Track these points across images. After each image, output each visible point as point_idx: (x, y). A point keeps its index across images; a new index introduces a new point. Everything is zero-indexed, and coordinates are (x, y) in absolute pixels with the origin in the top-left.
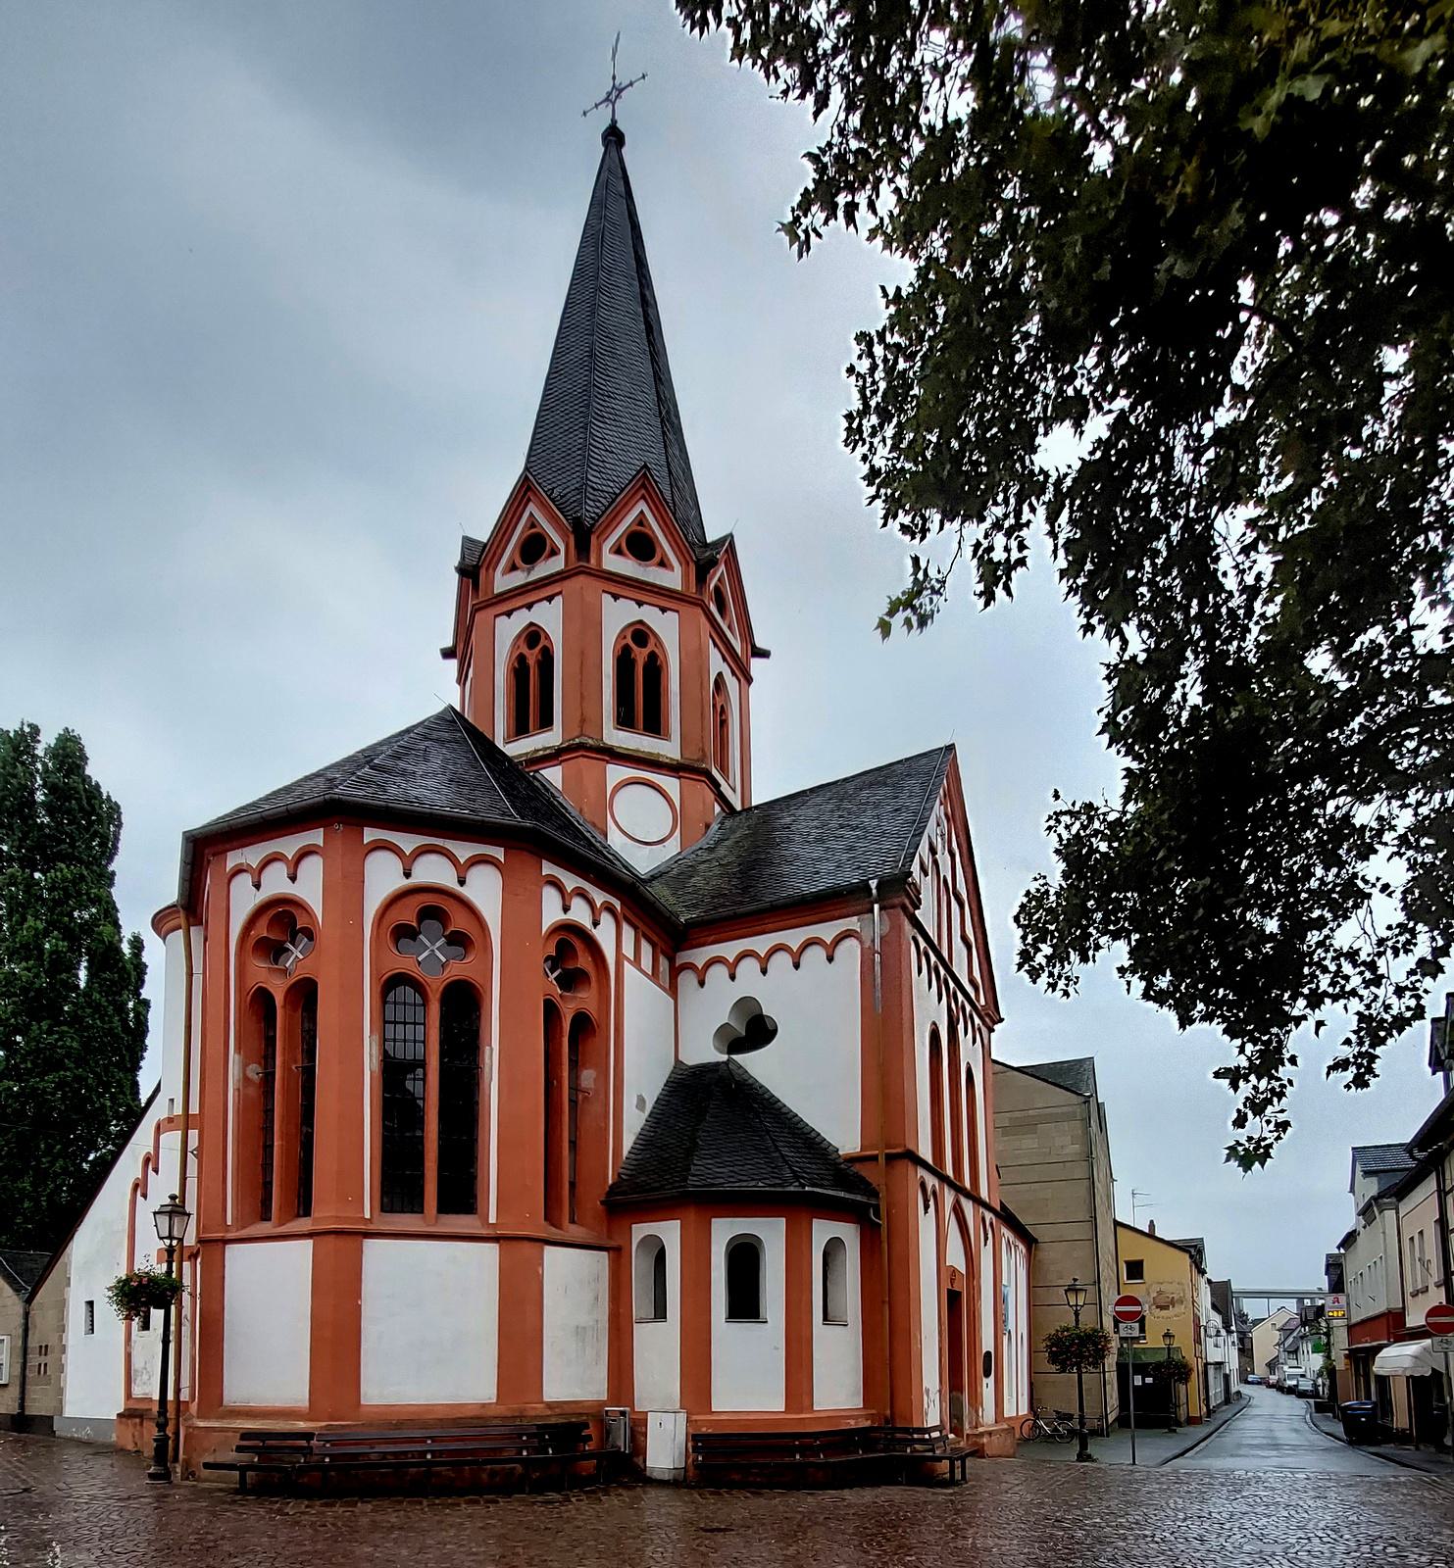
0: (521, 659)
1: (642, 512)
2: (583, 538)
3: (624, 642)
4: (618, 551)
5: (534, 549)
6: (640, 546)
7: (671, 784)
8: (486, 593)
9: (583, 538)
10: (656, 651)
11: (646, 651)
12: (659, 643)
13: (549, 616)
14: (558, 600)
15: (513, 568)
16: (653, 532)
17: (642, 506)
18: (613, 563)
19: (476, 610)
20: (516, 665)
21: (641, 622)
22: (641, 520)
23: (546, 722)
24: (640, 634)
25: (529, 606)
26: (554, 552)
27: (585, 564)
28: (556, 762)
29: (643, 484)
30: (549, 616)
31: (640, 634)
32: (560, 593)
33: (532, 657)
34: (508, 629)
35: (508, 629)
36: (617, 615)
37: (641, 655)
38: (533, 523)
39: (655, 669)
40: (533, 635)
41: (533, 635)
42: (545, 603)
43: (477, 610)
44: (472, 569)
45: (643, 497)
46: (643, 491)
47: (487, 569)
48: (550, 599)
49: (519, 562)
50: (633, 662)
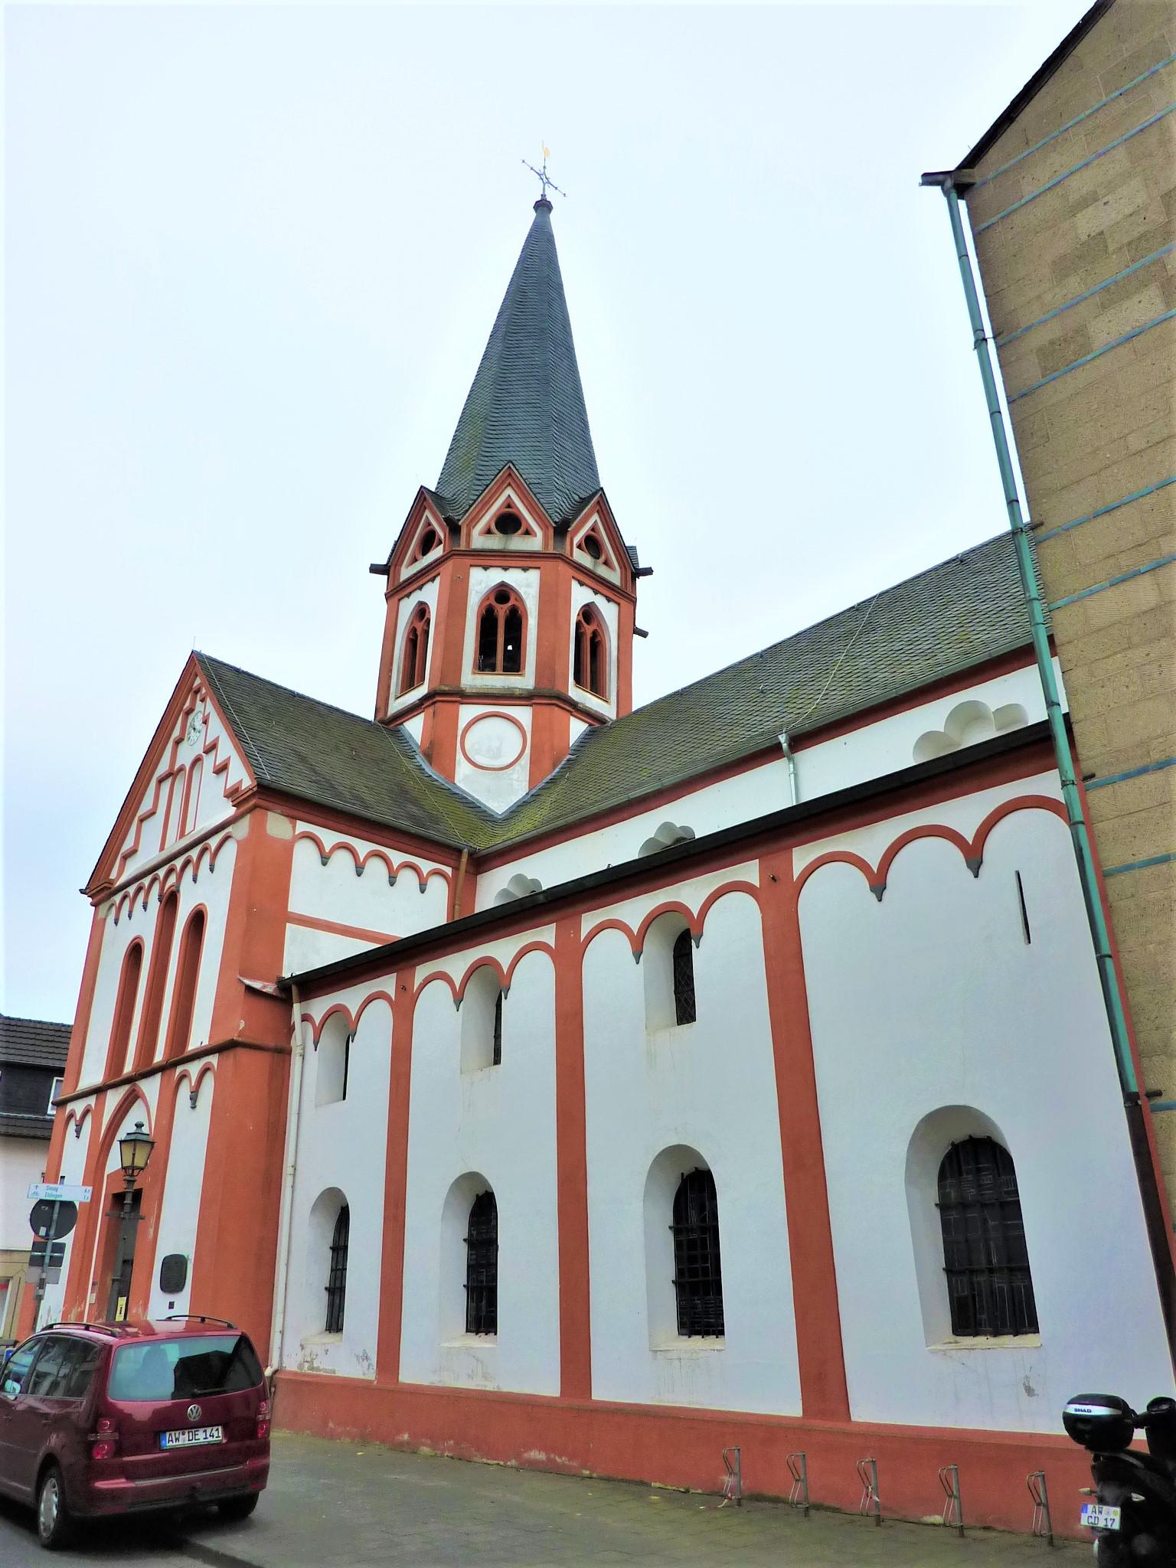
3: (488, 603)
7: (524, 714)
10: (516, 603)
12: (519, 598)
13: (430, 594)
17: (509, 491)
24: (503, 593)
31: (503, 593)
32: (439, 574)
36: (482, 581)
37: (502, 611)
39: (516, 622)
48: (433, 580)
50: (496, 620)
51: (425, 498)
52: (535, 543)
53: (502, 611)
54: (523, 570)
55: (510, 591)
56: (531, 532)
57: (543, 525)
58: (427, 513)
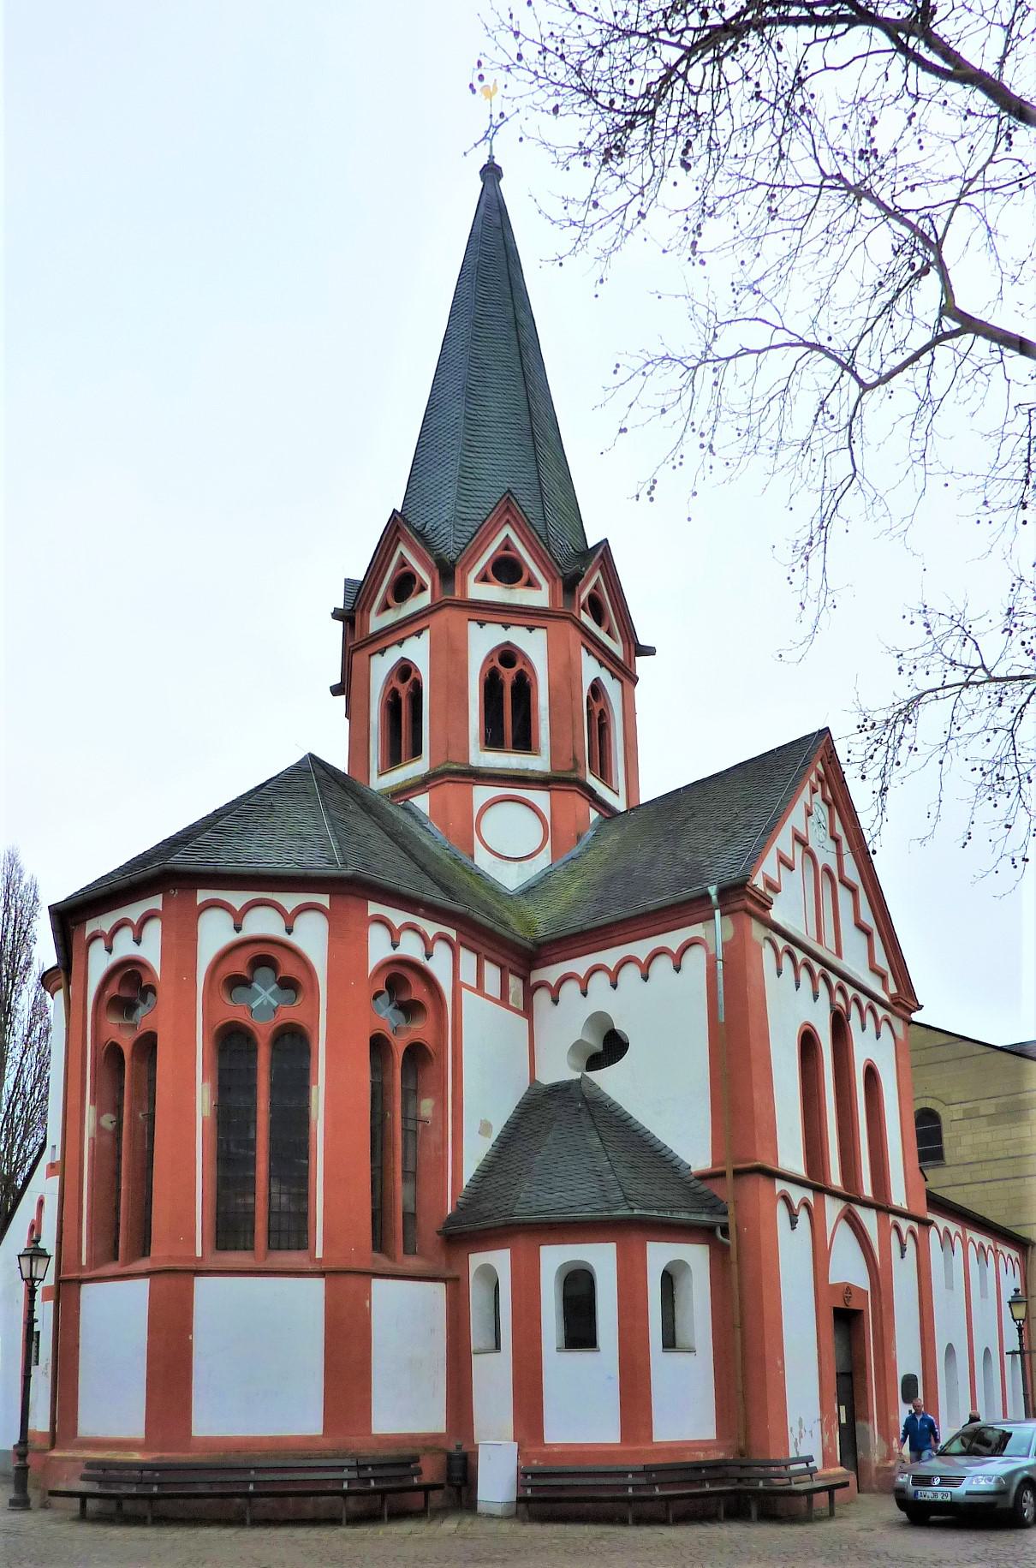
0: (394, 693)
1: (507, 536)
2: (447, 572)
4: (484, 579)
5: (405, 586)
6: (507, 570)
9: (447, 572)
13: (417, 650)
14: (426, 634)
15: (386, 607)
18: (478, 592)
22: (507, 544)
23: (416, 752)
24: (507, 655)
26: (423, 589)
30: (417, 650)
31: (507, 655)
32: (428, 627)
33: (404, 689)
34: (381, 667)
35: (381, 667)
37: (508, 676)
38: (403, 563)
39: (523, 688)
40: (405, 670)
42: (414, 638)
45: (508, 521)
47: (362, 612)
48: (418, 634)
49: (392, 602)
51: (398, 527)
53: (508, 676)
58: (402, 548)
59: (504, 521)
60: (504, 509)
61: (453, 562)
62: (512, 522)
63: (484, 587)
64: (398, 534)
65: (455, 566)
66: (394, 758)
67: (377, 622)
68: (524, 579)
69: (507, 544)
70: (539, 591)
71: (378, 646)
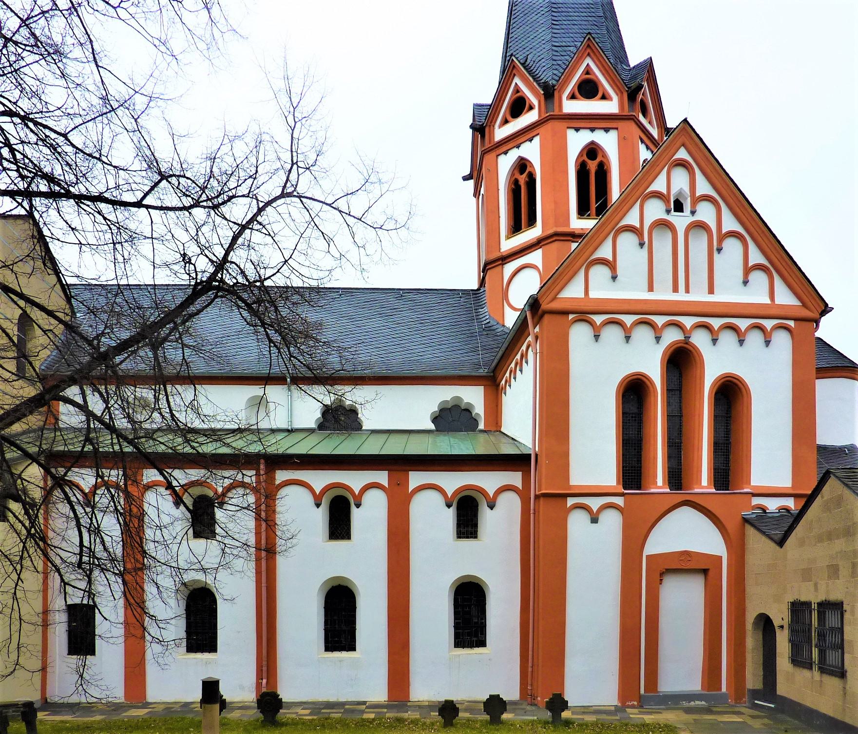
0: (516, 182)
1: (588, 64)
2: (549, 93)
3: (581, 160)
4: (573, 97)
5: (519, 107)
6: (588, 89)
8: (490, 143)
9: (549, 93)
11: (596, 162)
12: (605, 155)
13: (531, 151)
14: (537, 140)
15: (506, 122)
16: (596, 77)
17: (588, 61)
18: (571, 107)
19: (484, 153)
20: (513, 186)
21: (593, 141)
22: (588, 71)
23: (532, 221)
24: (592, 151)
25: (518, 147)
26: (531, 108)
27: (552, 113)
28: (538, 247)
29: (590, 47)
30: (531, 151)
31: (592, 151)
32: (538, 134)
33: (522, 179)
34: (506, 163)
35: (506, 163)
37: (592, 166)
38: (517, 90)
39: (603, 173)
40: (522, 165)
41: (522, 165)
42: (528, 143)
43: (484, 154)
44: (480, 129)
45: (589, 55)
46: (589, 50)
47: (490, 126)
48: (531, 140)
49: (509, 118)
51: (514, 67)
52: (611, 107)
53: (592, 166)
54: (605, 131)
55: (599, 150)
56: (607, 96)
57: (619, 92)
58: (517, 80)
59: (587, 53)
60: (586, 45)
61: (554, 86)
62: (592, 54)
63: (574, 103)
64: (514, 71)
65: (554, 90)
66: (516, 228)
67: (501, 133)
68: (600, 95)
69: (588, 71)
70: (611, 102)
71: (504, 149)
